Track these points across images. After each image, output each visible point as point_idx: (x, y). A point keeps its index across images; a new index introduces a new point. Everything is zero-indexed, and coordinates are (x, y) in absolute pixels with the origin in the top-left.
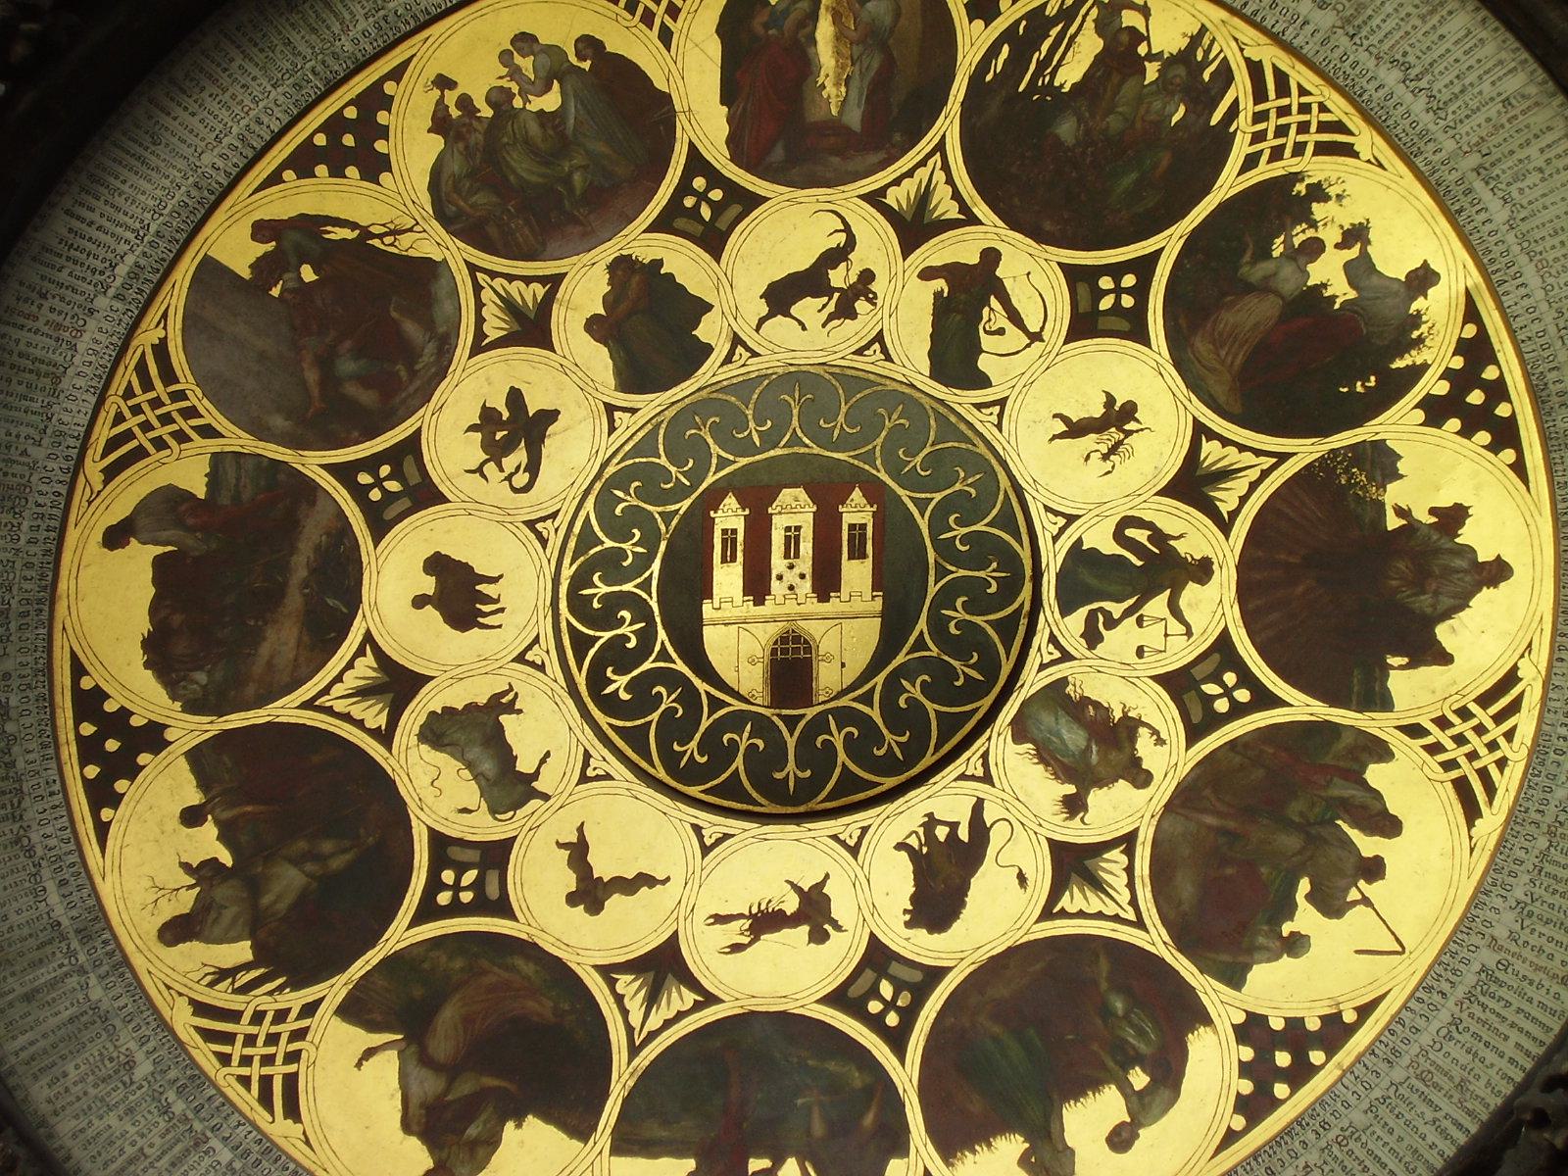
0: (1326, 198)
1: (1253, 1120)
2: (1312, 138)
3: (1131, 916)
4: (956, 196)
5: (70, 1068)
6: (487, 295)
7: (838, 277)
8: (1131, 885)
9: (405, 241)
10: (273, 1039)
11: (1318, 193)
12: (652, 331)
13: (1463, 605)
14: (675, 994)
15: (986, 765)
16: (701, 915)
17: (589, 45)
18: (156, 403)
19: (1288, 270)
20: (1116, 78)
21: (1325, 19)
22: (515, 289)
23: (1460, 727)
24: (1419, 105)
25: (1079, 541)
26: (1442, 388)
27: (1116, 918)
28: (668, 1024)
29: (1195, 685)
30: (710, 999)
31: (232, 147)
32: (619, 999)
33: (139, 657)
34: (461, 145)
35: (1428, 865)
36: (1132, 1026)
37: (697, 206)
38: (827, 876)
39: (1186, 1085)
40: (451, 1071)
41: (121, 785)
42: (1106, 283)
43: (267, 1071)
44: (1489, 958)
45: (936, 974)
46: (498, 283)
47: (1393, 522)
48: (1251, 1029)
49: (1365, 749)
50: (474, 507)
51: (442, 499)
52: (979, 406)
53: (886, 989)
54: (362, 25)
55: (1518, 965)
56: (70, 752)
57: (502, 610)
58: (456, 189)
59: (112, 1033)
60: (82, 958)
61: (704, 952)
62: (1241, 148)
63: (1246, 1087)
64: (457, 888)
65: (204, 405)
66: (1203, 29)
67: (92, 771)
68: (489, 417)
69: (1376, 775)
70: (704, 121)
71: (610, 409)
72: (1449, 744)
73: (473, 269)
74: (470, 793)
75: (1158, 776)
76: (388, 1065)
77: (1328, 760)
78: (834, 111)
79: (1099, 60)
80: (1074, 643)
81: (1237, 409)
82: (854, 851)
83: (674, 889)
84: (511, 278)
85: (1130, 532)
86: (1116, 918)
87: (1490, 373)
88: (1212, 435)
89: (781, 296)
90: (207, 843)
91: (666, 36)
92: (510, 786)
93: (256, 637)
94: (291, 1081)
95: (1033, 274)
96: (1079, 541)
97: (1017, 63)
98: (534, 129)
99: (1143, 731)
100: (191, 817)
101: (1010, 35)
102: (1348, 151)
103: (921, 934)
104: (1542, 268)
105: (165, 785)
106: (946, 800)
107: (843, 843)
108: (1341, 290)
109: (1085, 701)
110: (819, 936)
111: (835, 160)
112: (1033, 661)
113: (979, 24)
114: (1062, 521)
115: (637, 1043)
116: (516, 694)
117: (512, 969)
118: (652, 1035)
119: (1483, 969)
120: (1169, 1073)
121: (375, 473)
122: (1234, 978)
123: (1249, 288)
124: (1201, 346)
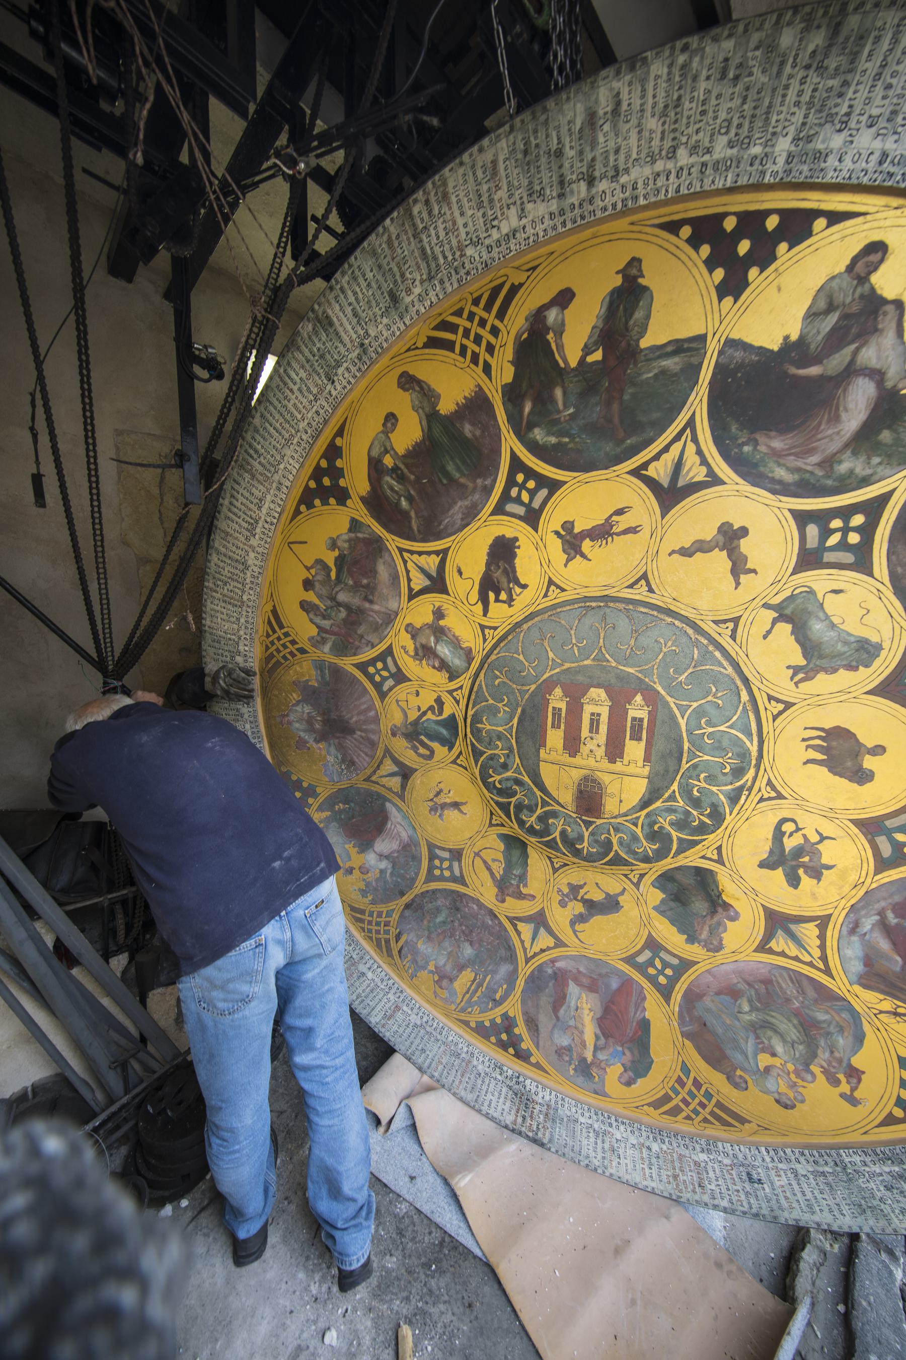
4: (519, 933)
6: (817, 953)
7: (579, 908)
8: (408, 572)
11: (364, 893)
14: (662, 472)
16: (645, 533)
21: (362, 968)
22: (793, 951)
25: (450, 749)
26: (310, 800)
27: (412, 552)
30: (635, 473)
32: (704, 462)
36: (396, 492)
38: (566, 565)
44: (254, 542)
45: (499, 510)
46: (807, 959)
48: (342, 496)
50: (829, 814)
51: (860, 824)
53: (525, 497)
55: (243, 539)
57: (804, 740)
68: (816, 873)
71: (720, 861)
74: (832, 605)
77: (333, 638)
80: (446, 698)
81: (388, 805)
82: (551, 582)
86: (412, 552)
89: (611, 905)
92: (794, 614)
96: (450, 749)
99: (412, 653)
101: (498, 1003)
103: (509, 534)
107: (558, 587)
109: (439, 669)
110: (568, 526)
115: (688, 430)
116: (792, 679)
117: (793, 470)
120: (375, 466)
122: (355, 525)
123: (387, 857)
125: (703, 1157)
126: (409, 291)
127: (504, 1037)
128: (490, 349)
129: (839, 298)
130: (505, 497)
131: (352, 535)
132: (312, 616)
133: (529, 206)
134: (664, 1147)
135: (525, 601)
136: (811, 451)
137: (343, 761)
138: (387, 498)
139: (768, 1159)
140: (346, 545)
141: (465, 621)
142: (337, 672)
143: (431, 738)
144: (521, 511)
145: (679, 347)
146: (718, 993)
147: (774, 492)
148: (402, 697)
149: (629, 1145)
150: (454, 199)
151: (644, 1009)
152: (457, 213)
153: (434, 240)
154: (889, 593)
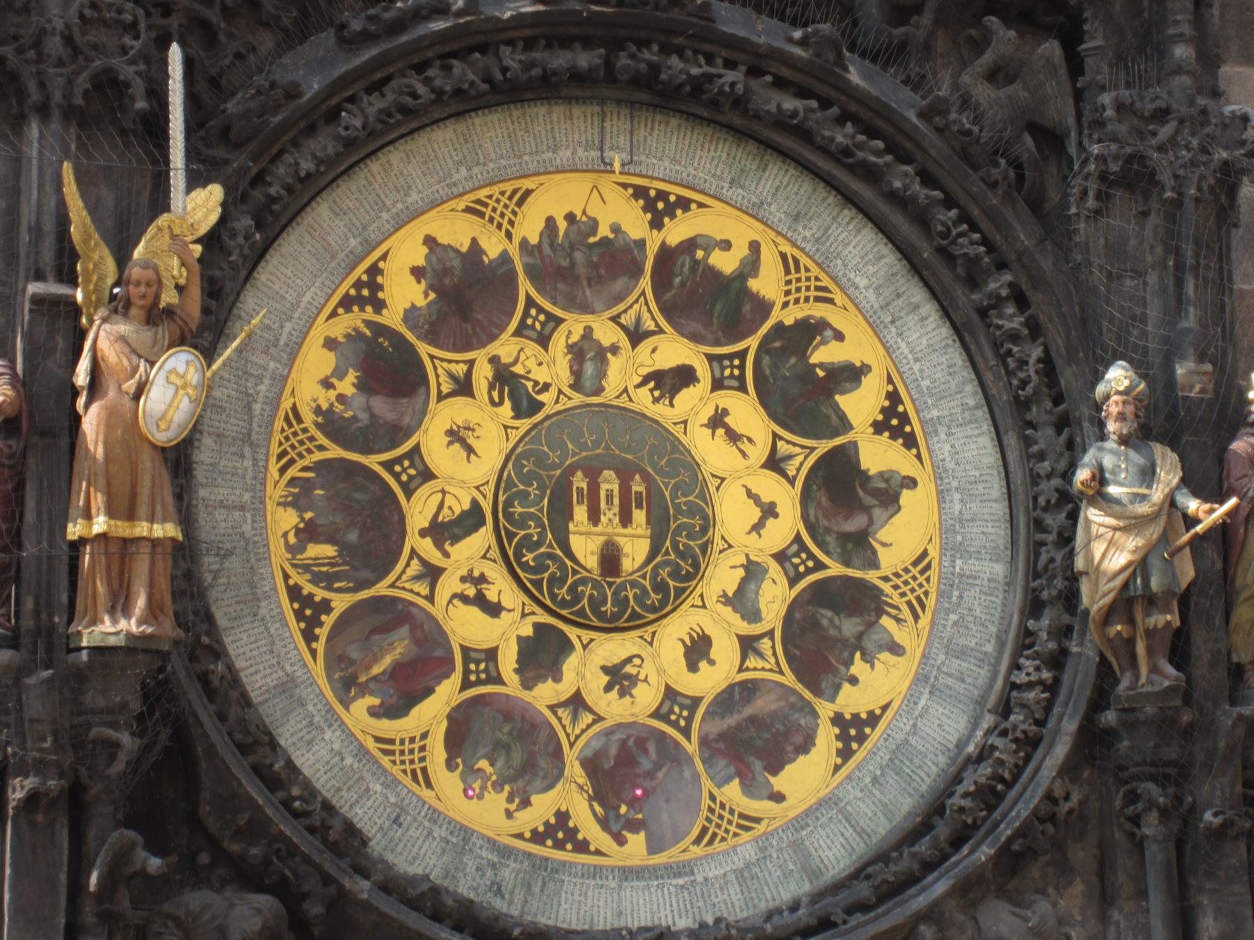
0: (319, 407)
1: (689, 201)
2: (297, 427)
3: (642, 299)
4: (408, 565)
5: (973, 644)
6: (577, 731)
7: (471, 592)
8: (631, 307)
9: (581, 781)
10: (906, 583)
11: (318, 411)
12: (543, 654)
13: (450, 246)
15: (621, 394)
16: (747, 463)
17: (450, 765)
18: (718, 826)
19: (355, 404)
20: (320, 529)
21: (247, 450)
22: (567, 722)
23: (497, 218)
24: (262, 388)
25: (513, 418)
26: (369, 309)
28: (794, 444)
29: (540, 333)
30: (775, 436)
31: (601, 878)
32: (798, 470)
33: (814, 751)
34: (528, 788)
35: (557, 199)
37: (483, 671)
39: (691, 235)
40: (867, 509)
41: (864, 716)
42: (404, 478)
43: (918, 575)
44: (580, 152)
45: (710, 358)
47: (432, 296)
48: (656, 224)
49: (526, 249)
50: (661, 672)
51: (668, 687)
52: (485, 497)
53: (727, 372)
54: (513, 865)
56: (868, 744)
58: (545, 777)
59: (950, 640)
60: (934, 673)
61: (759, 453)
62: (318, 456)
63: (679, 212)
64: (803, 562)
65: (704, 807)
66: (279, 504)
67: (868, 730)
68: (623, 693)
69: (534, 239)
70: (446, 694)
71: (585, 647)
72: (506, 219)
73: (572, 745)
74: (766, 585)
75: (583, 325)
76: (883, 535)
77: (539, 262)
78: (407, 642)
79: (319, 542)
80: (553, 392)
81: (423, 389)
82: (685, 422)
83: (742, 481)
84: (564, 727)
85: (497, 400)
86: (646, 303)
87: (353, 292)
88: (439, 392)
89: (494, 610)
90: (859, 667)
91: (424, 736)
92: (753, 571)
93: (773, 715)
94: (915, 564)
95: (419, 511)
96: (513, 418)
97: (337, 577)
98: (499, 764)
99: (570, 342)
100: (854, 681)
101: (329, 588)
102: (294, 408)
103: (699, 374)
104: (302, 295)
105: (851, 700)
106: (643, 400)
108: (352, 376)
109: (572, 372)
110: (725, 412)
111: (426, 627)
112: (570, 404)
113: (333, 604)
114: (509, 431)
117: (817, 518)
118: (803, 447)
119: (586, 150)
120: (690, 245)
121: (677, 720)
122: (641, 244)
123: (372, 416)
124: (406, 421)
125: (378, 788)
126: (805, 227)
127: (308, 612)
128: (797, 301)
129: (892, 482)
130: (720, 358)
131: (632, 245)
132: (546, 232)
133: (871, 290)
134: (356, 765)
135: (661, 412)
136: (828, 519)
137: (432, 324)
138: (674, 264)
139: (423, 814)
140: (622, 242)
141: (623, 374)
142: (511, 277)
143: (511, 397)
144: (718, 374)
145: (843, 418)
146: (498, 711)
147: (802, 516)
148: (528, 351)
149: (329, 747)
150: (859, 237)
151: (439, 683)
152: (853, 243)
153: (836, 234)
154: (788, 601)
